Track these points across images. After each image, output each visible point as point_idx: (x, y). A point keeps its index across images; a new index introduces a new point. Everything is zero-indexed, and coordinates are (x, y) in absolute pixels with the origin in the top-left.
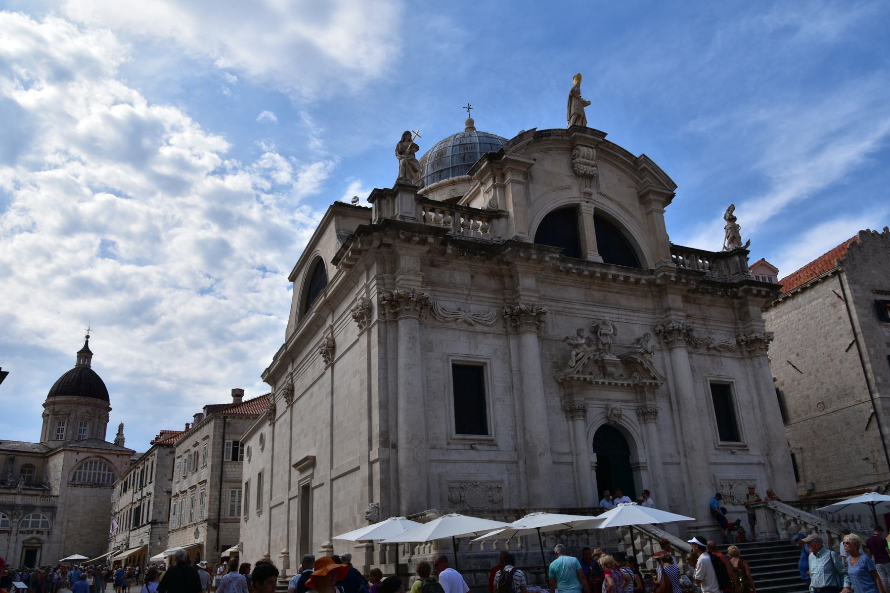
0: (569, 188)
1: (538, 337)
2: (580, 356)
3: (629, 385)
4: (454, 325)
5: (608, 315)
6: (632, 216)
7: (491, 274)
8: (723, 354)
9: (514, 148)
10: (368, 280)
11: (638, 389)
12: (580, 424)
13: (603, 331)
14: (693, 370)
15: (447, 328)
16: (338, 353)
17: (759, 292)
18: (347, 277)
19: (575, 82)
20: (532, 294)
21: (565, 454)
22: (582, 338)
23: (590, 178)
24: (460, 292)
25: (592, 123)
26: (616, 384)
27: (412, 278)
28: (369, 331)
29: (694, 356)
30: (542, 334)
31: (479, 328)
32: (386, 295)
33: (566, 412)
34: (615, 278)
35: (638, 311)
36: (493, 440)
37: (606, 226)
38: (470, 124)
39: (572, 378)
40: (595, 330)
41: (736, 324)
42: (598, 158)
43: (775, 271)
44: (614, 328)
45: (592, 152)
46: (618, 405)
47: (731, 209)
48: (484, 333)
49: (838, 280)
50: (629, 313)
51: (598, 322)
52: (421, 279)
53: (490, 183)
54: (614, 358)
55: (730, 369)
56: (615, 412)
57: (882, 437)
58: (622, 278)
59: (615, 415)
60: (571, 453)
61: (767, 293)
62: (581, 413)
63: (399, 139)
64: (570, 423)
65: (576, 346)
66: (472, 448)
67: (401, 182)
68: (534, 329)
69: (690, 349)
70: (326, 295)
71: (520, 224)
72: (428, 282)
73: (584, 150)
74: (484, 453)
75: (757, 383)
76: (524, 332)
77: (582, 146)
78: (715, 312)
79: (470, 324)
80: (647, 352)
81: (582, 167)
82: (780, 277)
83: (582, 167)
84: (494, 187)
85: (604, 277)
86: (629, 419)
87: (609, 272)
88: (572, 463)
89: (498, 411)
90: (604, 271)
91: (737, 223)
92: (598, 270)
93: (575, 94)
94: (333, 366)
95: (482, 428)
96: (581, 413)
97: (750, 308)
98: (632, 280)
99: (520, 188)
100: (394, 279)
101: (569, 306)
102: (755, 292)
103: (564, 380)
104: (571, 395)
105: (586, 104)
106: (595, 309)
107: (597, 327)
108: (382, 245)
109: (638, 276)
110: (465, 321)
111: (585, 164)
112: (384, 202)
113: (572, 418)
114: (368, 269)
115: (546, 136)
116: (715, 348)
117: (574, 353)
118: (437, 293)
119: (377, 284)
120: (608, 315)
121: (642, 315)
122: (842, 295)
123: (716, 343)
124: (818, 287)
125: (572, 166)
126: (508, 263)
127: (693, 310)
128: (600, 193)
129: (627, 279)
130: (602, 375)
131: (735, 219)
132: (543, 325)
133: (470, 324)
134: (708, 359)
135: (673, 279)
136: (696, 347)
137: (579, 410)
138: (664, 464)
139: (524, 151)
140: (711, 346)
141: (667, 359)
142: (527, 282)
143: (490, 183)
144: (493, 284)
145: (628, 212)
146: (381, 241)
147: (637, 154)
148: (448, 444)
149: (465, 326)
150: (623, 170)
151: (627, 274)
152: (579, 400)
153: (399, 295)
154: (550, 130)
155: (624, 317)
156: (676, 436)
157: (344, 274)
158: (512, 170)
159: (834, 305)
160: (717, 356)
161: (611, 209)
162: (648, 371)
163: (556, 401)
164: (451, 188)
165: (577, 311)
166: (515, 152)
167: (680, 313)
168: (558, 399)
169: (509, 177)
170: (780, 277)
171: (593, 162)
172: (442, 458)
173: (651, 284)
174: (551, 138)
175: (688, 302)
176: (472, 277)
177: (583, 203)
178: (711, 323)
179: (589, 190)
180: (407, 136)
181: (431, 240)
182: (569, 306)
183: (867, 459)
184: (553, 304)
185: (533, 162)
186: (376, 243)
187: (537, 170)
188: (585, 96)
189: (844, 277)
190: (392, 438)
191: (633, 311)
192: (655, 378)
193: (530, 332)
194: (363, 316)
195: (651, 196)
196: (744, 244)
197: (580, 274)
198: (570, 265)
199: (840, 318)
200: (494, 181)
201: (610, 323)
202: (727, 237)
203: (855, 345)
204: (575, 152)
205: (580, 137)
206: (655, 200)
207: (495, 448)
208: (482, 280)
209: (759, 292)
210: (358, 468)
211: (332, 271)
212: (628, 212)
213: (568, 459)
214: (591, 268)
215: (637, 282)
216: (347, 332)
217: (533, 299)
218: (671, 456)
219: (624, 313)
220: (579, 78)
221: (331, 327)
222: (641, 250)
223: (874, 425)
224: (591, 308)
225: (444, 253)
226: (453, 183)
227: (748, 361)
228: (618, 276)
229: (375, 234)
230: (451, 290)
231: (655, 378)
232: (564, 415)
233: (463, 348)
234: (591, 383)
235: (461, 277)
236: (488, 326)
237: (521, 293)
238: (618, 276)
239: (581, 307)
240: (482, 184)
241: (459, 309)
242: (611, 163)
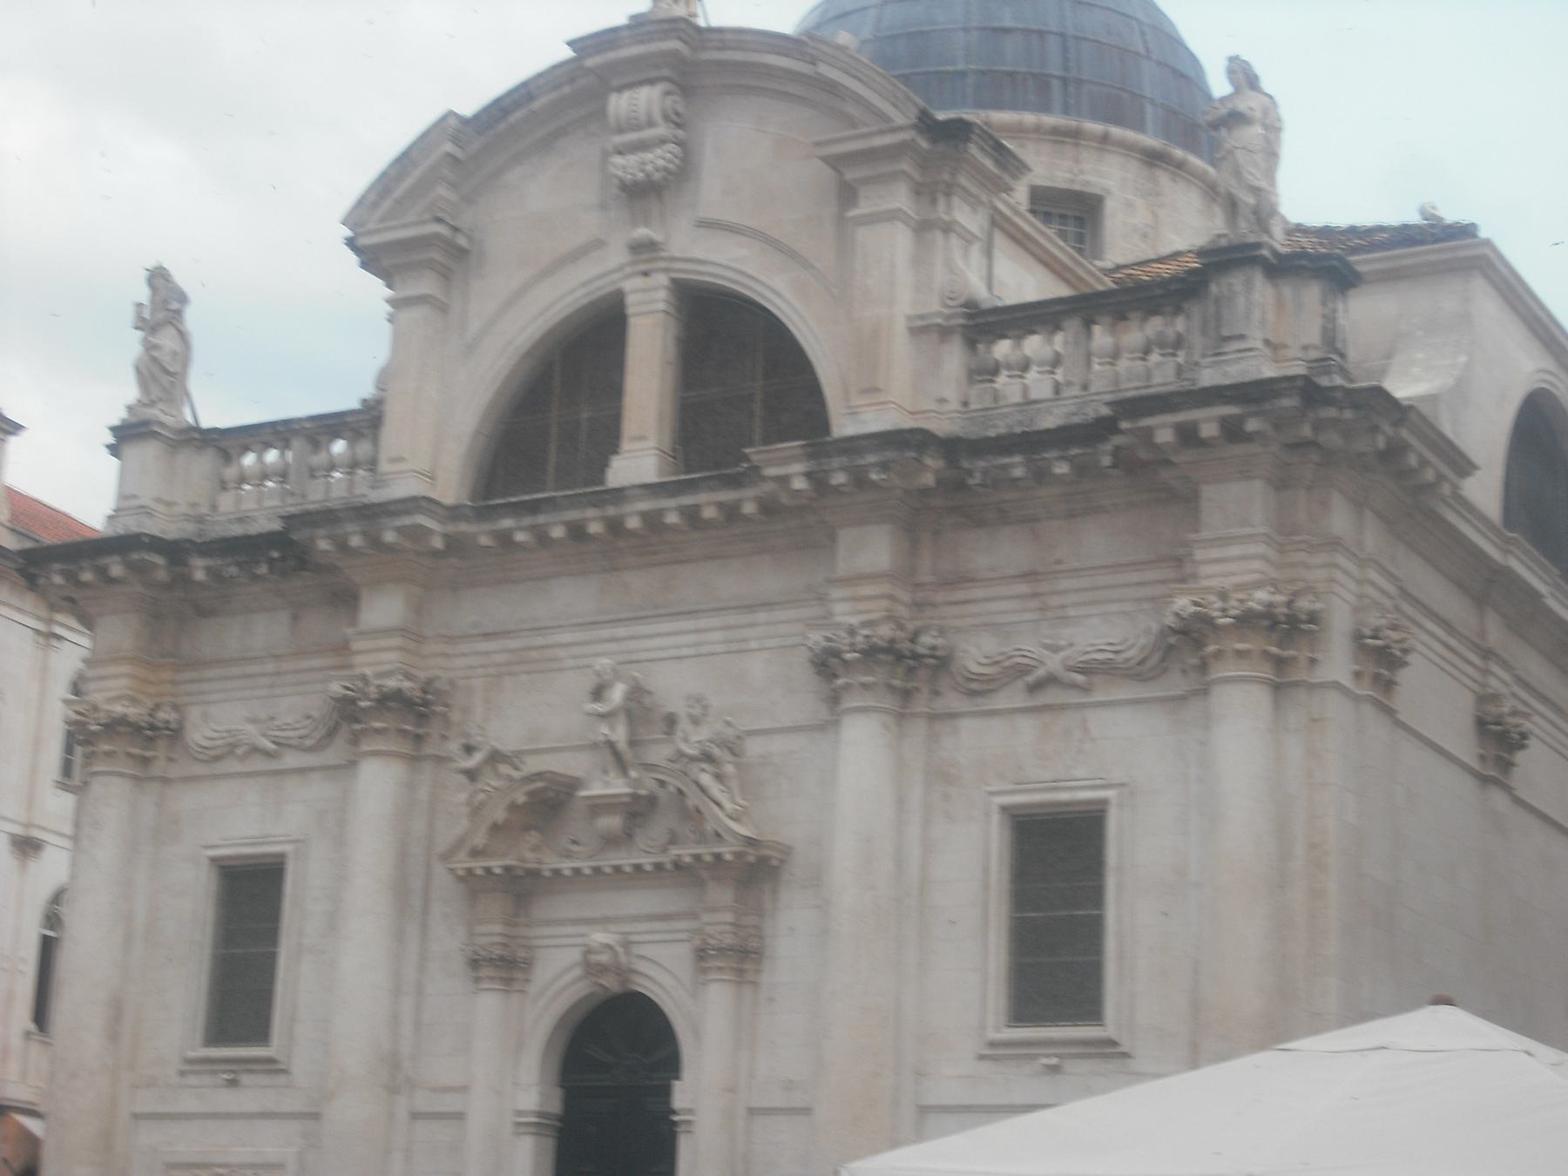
3: (659, 867)
4: (232, 766)
6: (805, 263)
8: (1099, 697)
12: (489, 1004)
14: (941, 775)
17: (1188, 436)
20: (382, 643)
24: (256, 669)
26: (618, 869)
29: (966, 724)
31: (291, 760)
35: (768, 605)
36: (271, 1061)
44: (637, 693)
45: (646, 99)
46: (599, 937)
48: (301, 771)
50: (732, 619)
54: (618, 787)
55: (1117, 755)
58: (672, 518)
59: (603, 969)
60: (464, 1089)
61: (1232, 431)
63: (143, 294)
65: (472, 775)
66: (233, 1083)
69: (953, 701)
73: (620, 104)
74: (253, 1095)
77: (620, 89)
79: (268, 754)
86: (665, 974)
87: (628, 508)
88: (459, 1116)
89: (297, 982)
90: (611, 511)
92: (591, 513)
95: (261, 1034)
101: (540, 641)
102: (1165, 436)
106: (621, 631)
107: (598, 693)
110: (255, 750)
115: (518, 105)
116: (1051, 680)
118: (206, 686)
121: (780, 615)
123: (1054, 663)
129: (692, 516)
133: (268, 754)
134: (1027, 727)
135: (799, 484)
136: (973, 694)
140: (1041, 672)
142: (383, 609)
145: (792, 254)
148: (182, 1073)
149: (259, 764)
154: (525, 84)
155: (717, 636)
160: (1062, 708)
163: (449, 939)
165: (561, 653)
171: (662, 130)
172: (161, 1109)
173: (769, 508)
174: (536, 105)
175: (980, 523)
176: (295, 618)
177: (628, 285)
178: (1065, 584)
179: (642, 232)
180: (158, 278)
181: (116, 570)
182: (540, 641)
191: (750, 608)
197: (543, 539)
198: (507, 523)
205: (613, 67)
206: (867, 181)
207: (282, 1079)
209: (1188, 436)
212: (792, 254)
213: (449, 1103)
215: (731, 513)
217: (385, 656)
219: (716, 621)
224: (605, 633)
230: (235, 670)
233: (239, 819)
235: (265, 630)
236: (310, 750)
238: (660, 513)
239: (579, 636)
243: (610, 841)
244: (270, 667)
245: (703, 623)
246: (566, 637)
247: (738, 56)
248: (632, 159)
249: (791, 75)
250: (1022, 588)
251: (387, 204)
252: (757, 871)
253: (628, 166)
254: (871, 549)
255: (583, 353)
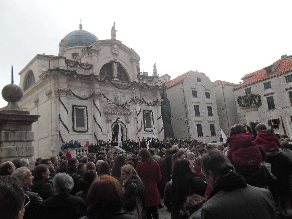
0: (110, 57)
1: (99, 101)
2: (111, 106)
3: (123, 114)
5: (119, 95)
7: (87, 83)
9: (95, 46)
10: (50, 84)
11: (126, 115)
13: (117, 99)
15: (74, 99)
16: (40, 103)
18: (42, 82)
19: (112, 25)
21: (105, 132)
22: (111, 101)
23: (116, 55)
25: (117, 38)
27: (64, 85)
28: (51, 99)
30: (101, 100)
32: (56, 89)
33: (106, 121)
34: (121, 84)
37: (121, 69)
38: (81, 26)
39: (108, 112)
40: (115, 99)
41: (153, 97)
42: (119, 48)
43: (170, 77)
44: (120, 98)
45: (117, 47)
47: (155, 64)
49: (182, 84)
51: (116, 96)
52: (67, 85)
53: (87, 55)
56: (119, 121)
57: (188, 126)
58: (123, 85)
62: (110, 122)
64: (107, 124)
65: (110, 104)
67: (61, 56)
68: (98, 99)
69: (141, 104)
70: (35, 85)
71: (97, 71)
72: (69, 86)
73: (115, 46)
75: (157, 113)
76: (96, 100)
78: (148, 94)
80: (128, 105)
81: (114, 51)
82: (171, 79)
83: (114, 51)
84: (88, 56)
85: (118, 84)
90: (118, 83)
91: (156, 68)
92: (117, 82)
93: (113, 29)
94: (38, 106)
96: (110, 122)
97: (157, 93)
98: (126, 85)
99: (95, 58)
100: (59, 84)
101: (108, 92)
103: (106, 113)
104: (108, 117)
105: (116, 31)
107: (116, 98)
108: (55, 75)
109: (128, 84)
111: (115, 50)
112: (55, 61)
113: (108, 122)
114: (50, 80)
115: (104, 41)
117: (109, 105)
119: (54, 86)
120: (119, 95)
122: (182, 88)
124: (178, 85)
125: (112, 50)
126: (92, 80)
127: (143, 93)
128: (119, 59)
130: (116, 111)
131: (156, 67)
132: (101, 98)
134: (145, 106)
137: (109, 121)
138: (131, 134)
139: (97, 46)
141: (134, 107)
143: (87, 55)
144: (87, 86)
145: (127, 65)
146: (55, 73)
147: (130, 48)
150: (126, 52)
151: (125, 83)
152: (110, 118)
153: (60, 90)
156: (135, 126)
157: (42, 81)
158: (94, 52)
159: (181, 91)
161: (122, 64)
162: (128, 110)
164: (75, 50)
166: (95, 47)
167: (139, 94)
168: (104, 118)
169: (93, 54)
170: (171, 79)
174: (106, 42)
176: (81, 84)
179: (116, 58)
183: (184, 132)
184: (104, 91)
185: (100, 50)
186: (53, 74)
187: (101, 52)
188: (116, 29)
189: (184, 84)
190: (58, 129)
192: (130, 112)
193: (98, 100)
194: (49, 94)
195: (133, 61)
196: (158, 75)
199: (182, 95)
200: (88, 55)
201: (119, 97)
202: (154, 72)
203: (184, 103)
204: (113, 47)
206: (134, 62)
208: (84, 85)
210: (48, 137)
211: (37, 79)
212: (127, 65)
214: (115, 82)
216: (43, 98)
218: (133, 132)
220: (114, 23)
221: (37, 95)
222: (130, 77)
223: (187, 123)
225: (74, 77)
226: (75, 48)
227: (156, 107)
228: (122, 84)
229: (53, 72)
231: (130, 112)
232: (106, 122)
234: (113, 113)
235: (78, 84)
237: (95, 89)
238: (122, 84)
240: (85, 54)
241: (78, 93)
242: (123, 50)
243: (119, 111)
244: (80, 88)
245: (122, 94)
246: (111, 92)
247: (123, 46)
248: (116, 52)
249: (126, 50)
250: (144, 96)
251: (95, 46)
252: (130, 115)
253: (116, 52)
254: (138, 91)
255: (108, 67)
